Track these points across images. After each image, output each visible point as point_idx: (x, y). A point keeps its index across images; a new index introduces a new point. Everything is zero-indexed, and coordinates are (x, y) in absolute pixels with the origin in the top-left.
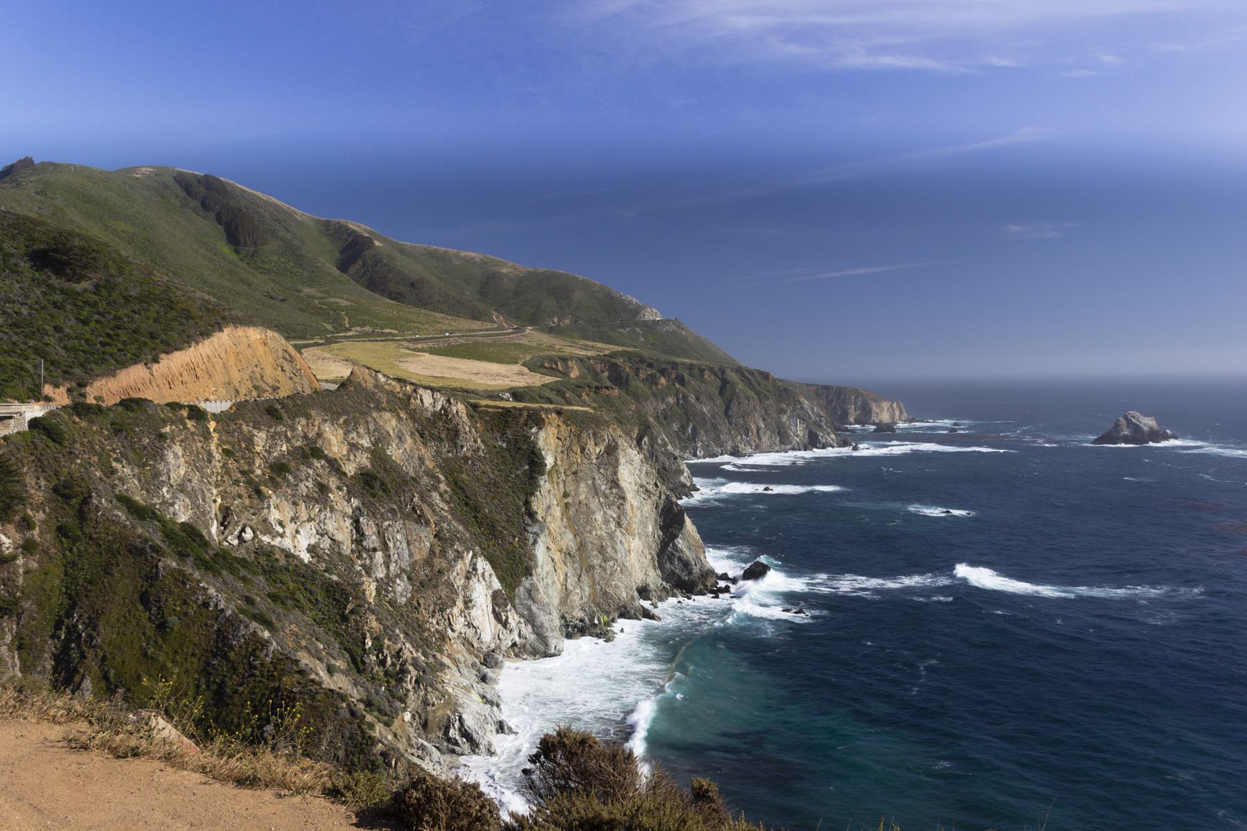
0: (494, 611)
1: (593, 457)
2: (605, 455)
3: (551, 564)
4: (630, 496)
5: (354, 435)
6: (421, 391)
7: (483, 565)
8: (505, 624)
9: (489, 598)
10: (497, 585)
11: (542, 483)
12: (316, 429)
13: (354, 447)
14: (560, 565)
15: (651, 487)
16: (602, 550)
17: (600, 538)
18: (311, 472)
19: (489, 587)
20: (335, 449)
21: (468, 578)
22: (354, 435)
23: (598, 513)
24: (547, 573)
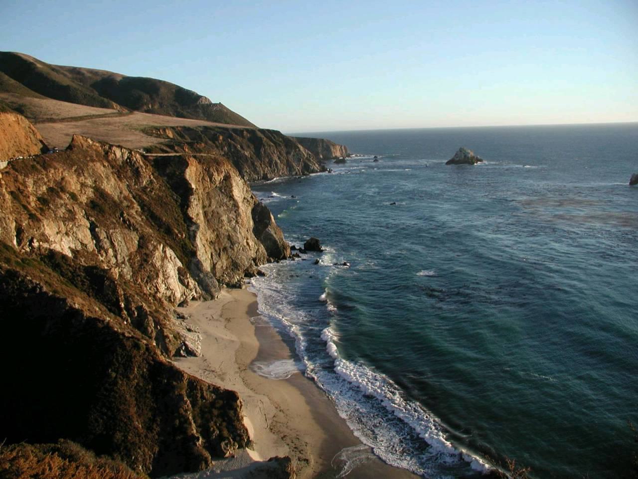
0: (179, 278)
1: (217, 183)
2: (224, 182)
3: (203, 249)
4: (240, 204)
5: (83, 178)
6: (114, 148)
7: (169, 252)
8: (187, 286)
9: (177, 272)
10: (180, 264)
11: (192, 200)
12: (61, 175)
13: (83, 185)
14: (208, 249)
15: (249, 199)
16: (229, 238)
17: (228, 231)
18: (62, 202)
19: (175, 265)
20: (73, 188)
21: (163, 260)
22: (83, 178)
23: (224, 216)
24: (203, 254)
